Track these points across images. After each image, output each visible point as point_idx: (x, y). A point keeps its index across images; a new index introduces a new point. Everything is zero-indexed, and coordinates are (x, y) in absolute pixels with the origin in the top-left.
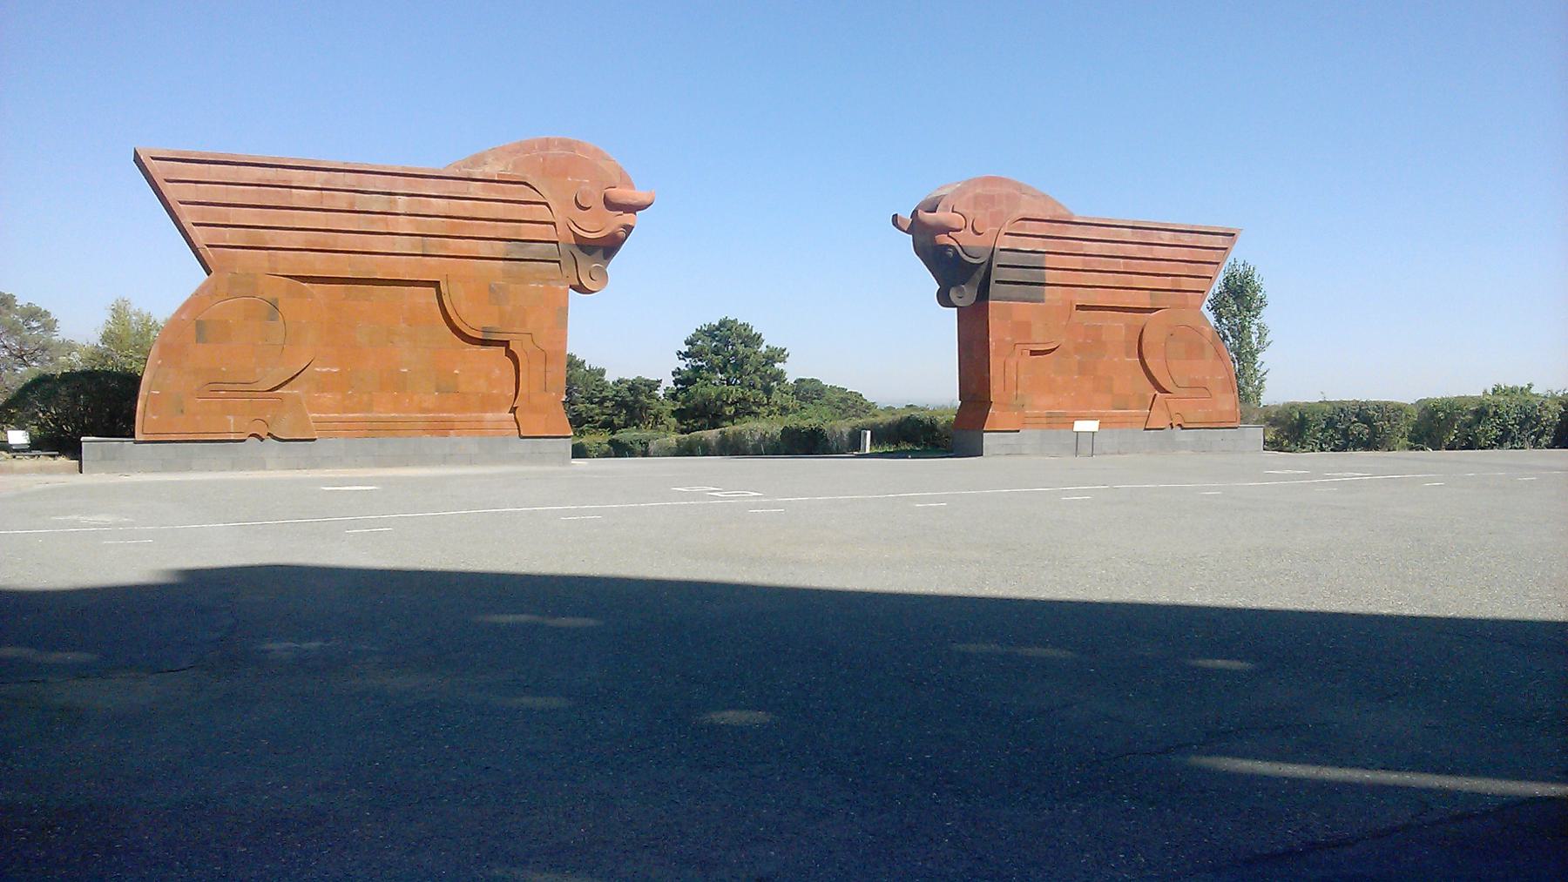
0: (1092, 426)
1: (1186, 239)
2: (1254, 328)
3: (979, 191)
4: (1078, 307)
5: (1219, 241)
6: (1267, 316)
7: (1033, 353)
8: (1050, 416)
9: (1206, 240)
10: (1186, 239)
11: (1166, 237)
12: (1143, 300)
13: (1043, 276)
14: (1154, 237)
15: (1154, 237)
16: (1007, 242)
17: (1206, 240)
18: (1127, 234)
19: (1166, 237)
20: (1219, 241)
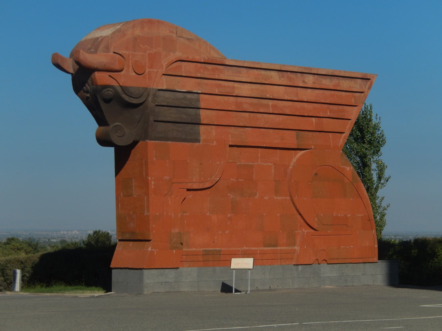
0: (247, 263)
1: (327, 83)
2: (374, 166)
3: (138, 32)
4: (230, 146)
5: (356, 85)
6: (386, 154)
7: (188, 190)
8: (206, 253)
9: (345, 84)
10: (327, 83)
11: (310, 80)
12: (290, 139)
13: (198, 115)
14: (298, 80)
15: (298, 80)
16: (164, 83)
17: (345, 84)
18: (275, 77)
19: (310, 80)
20: (356, 85)
